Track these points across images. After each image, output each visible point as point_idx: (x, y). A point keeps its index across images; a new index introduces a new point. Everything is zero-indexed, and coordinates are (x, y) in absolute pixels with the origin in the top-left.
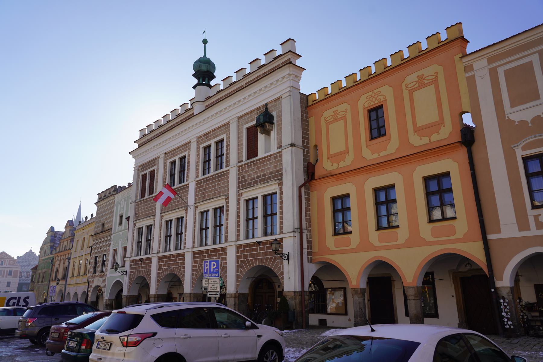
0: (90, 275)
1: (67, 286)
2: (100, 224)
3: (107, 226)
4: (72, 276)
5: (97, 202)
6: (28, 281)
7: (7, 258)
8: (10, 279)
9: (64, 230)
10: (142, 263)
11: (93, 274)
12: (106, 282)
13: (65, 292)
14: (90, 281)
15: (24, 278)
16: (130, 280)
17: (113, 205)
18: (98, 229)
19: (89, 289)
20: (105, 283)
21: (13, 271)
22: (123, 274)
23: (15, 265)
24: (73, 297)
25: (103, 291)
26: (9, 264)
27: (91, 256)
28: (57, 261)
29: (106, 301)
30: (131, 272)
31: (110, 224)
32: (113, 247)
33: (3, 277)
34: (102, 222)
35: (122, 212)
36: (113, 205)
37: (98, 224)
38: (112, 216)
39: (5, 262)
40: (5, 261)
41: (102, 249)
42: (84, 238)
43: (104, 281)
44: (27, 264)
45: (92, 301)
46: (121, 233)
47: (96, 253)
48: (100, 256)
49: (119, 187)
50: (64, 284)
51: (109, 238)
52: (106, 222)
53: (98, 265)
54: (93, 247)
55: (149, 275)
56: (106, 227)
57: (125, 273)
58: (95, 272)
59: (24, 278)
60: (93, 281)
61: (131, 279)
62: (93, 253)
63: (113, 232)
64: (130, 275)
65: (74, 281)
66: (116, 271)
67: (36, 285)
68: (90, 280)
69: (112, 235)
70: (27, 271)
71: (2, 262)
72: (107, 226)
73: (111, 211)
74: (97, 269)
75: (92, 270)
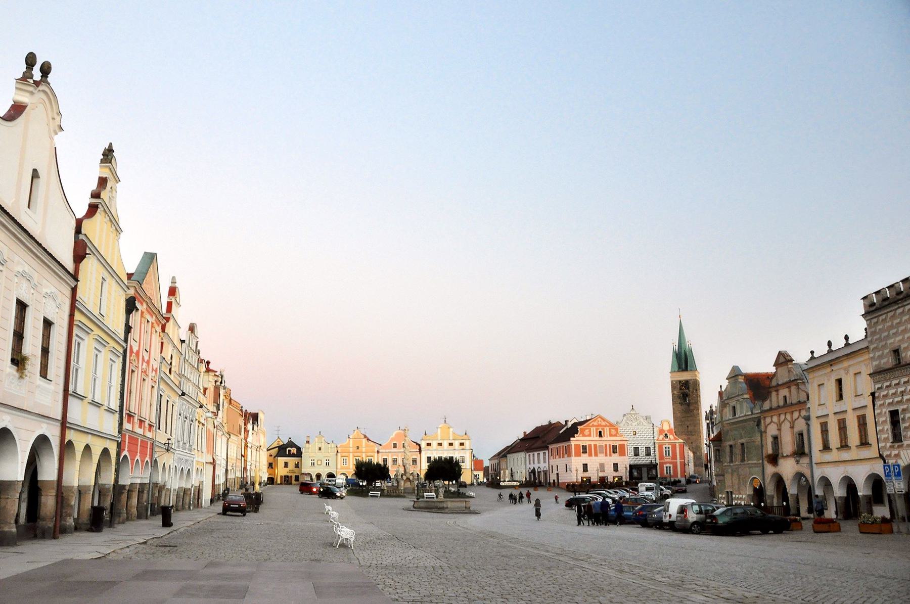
1: (814, 466)
2: (886, 351)
4: (842, 447)
5: (864, 313)
6: (647, 462)
7: (606, 426)
8: (616, 458)
9: (773, 370)
13: (812, 477)
15: (632, 456)
18: (885, 360)
21: (587, 447)
23: (618, 435)
24: (819, 481)
26: (611, 435)
27: (876, 412)
28: (784, 421)
33: (606, 456)
34: (895, 346)
37: (881, 352)
39: (604, 431)
40: (603, 429)
42: (839, 382)
44: (632, 432)
47: (890, 404)
48: (904, 410)
50: (809, 462)
52: (903, 346)
54: (876, 395)
59: (632, 456)
60: (897, 456)
62: (881, 405)
65: (834, 455)
67: (726, 466)
68: (885, 454)
70: (635, 445)
71: (600, 432)
74: (903, 434)
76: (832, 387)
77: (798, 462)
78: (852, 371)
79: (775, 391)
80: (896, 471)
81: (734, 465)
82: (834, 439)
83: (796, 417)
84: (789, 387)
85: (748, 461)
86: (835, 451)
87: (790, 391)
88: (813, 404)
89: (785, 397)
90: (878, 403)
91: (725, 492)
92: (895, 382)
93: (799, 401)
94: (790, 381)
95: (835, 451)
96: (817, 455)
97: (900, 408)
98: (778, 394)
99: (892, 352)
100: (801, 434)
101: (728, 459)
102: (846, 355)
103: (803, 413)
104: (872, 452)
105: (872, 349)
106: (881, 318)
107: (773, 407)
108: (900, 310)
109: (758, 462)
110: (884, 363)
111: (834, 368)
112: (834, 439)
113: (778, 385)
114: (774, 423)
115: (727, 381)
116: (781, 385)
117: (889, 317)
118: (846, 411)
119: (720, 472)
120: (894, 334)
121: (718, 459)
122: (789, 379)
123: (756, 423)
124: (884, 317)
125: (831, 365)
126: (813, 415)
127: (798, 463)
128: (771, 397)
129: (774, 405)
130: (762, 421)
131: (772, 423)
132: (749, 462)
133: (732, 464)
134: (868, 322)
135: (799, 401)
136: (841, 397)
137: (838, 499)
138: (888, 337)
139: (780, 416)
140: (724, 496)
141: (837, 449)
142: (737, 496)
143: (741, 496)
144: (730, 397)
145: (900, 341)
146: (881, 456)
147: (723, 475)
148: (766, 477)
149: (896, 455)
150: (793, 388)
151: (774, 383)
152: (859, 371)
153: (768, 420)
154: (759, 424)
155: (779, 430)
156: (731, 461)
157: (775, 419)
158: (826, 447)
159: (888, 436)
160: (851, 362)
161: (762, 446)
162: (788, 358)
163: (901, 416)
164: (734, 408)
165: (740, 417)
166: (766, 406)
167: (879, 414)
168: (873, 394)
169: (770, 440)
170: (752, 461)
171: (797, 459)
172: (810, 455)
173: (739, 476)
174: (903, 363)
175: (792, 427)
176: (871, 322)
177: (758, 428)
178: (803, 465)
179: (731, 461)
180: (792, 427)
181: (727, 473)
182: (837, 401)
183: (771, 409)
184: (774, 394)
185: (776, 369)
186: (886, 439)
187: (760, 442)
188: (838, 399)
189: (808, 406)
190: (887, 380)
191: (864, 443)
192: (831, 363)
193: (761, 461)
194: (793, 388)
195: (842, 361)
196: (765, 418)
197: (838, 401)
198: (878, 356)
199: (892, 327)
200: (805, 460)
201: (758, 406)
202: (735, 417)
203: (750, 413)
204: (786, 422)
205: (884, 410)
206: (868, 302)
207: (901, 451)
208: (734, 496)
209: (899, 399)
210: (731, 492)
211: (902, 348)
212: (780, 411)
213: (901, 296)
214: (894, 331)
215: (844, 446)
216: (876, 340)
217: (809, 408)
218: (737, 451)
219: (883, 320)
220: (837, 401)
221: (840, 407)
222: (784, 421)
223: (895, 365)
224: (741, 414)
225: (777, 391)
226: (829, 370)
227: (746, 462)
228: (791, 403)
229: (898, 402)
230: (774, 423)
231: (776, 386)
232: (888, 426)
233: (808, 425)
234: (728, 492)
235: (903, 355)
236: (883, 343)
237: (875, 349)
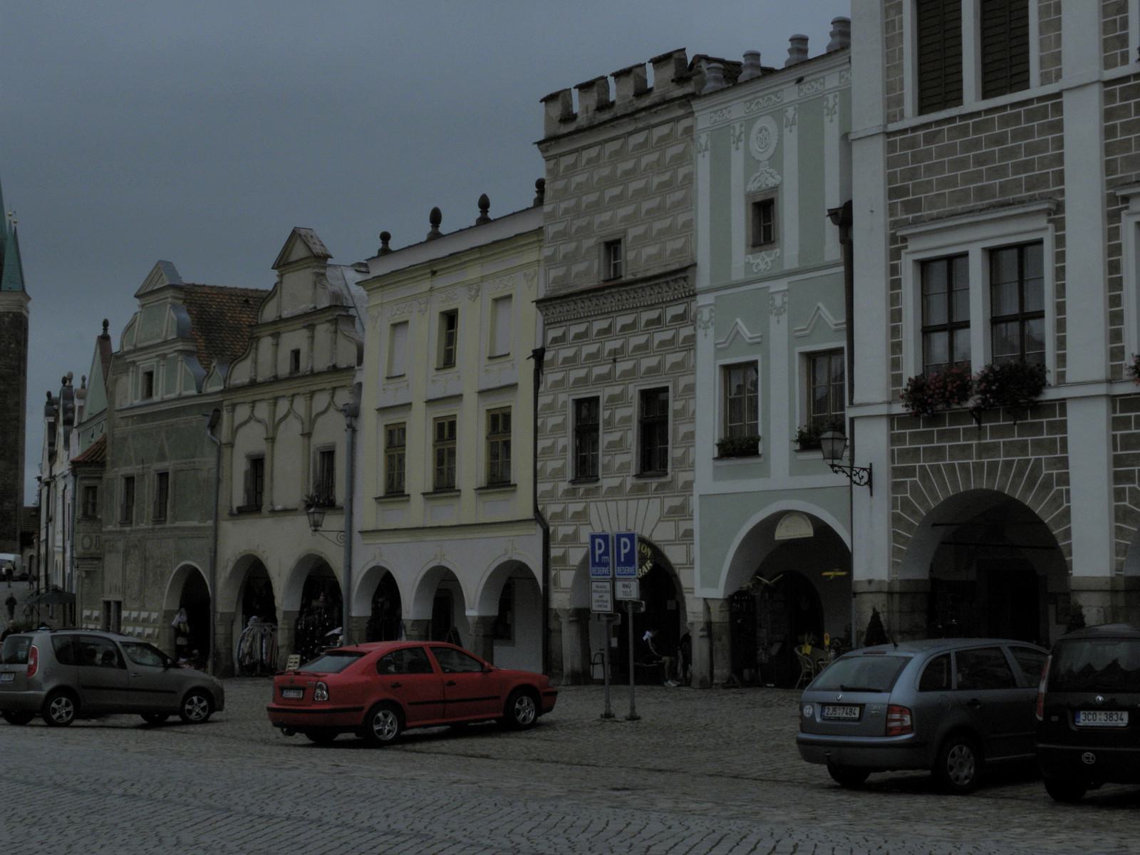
0: (555, 488)
1: (357, 537)
2: (589, 243)
3: (652, 250)
9: (264, 280)
10: (980, 428)
11: (573, 482)
12: (696, 515)
14: (559, 516)
16: (894, 506)
17: (672, 151)
18: (581, 267)
19: (555, 552)
20: (684, 526)
22: (858, 481)
25: (675, 555)
27: (542, 400)
28: (285, 417)
29: (708, 609)
30: (896, 472)
31: (678, 244)
32: (719, 351)
34: (610, 234)
35: (771, 182)
36: (672, 151)
37: (573, 245)
38: (687, 203)
41: (622, 367)
42: (450, 319)
43: (681, 512)
45: (580, 607)
46: (782, 285)
47: (580, 382)
48: (612, 399)
49: (699, 58)
51: (679, 309)
52: (632, 233)
53: (605, 439)
54: (548, 356)
55: (1047, 485)
56: (638, 260)
57: (865, 474)
58: (585, 469)
60: (581, 516)
61: (906, 504)
62: (557, 384)
63: (703, 278)
64: (896, 487)
66: (832, 466)
67: (110, 532)
68: (550, 509)
69: (698, 297)
72: (652, 250)
73: (666, 177)
74: (602, 460)
75: (567, 462)
76: (426, 330)
77: (316, 526)
78: (492, 290)
79: (272, 335)
80: (623, 551)
81: (131, 531)
82: (419, 472)
83: (322, 408)
84: (311, 327)
85: (175, 519)
86: (417, 500)
87: (312, 337)
88: (371, 375)
89: (296, 354)
90: (550, 377)
91: (102, 605)
92: (602, 324)
93: (334, 366)
94: (316, 312)
95: (417, 500)
96: (367, 513)
97: (604, 393)
98: (277, 345)
99: (602, 247)
100: (328, 455)
101: (118, 513)
102: (480, 248)
103: (343, 398)
104: (521, 505)
105: (551, 235)
106: (586, 155)
107: (258, 380)
108: (638, 138)
109: (202, 525)
110: (577, 275)
111: (440, 282)
112: (419, 472)
113: (280, 320)
114: (259, 421)
115: (137, 301)
116: (287, 320)
117: (607, 153)
118: (459, 397)
119: (93, 550)
120: (613, 199)
121: (90, 512)
122: (312, 305)
123: (207, 420)
124: (593, 152)
125: (434, 273)
126: (369, 405)
127: (315, 531)
128: (257, 349)
129: (264, 374)
130: (225, 416)
131: (252, 423)
132: (177, 524)
133: (127, 529)
134: (553, 162)
135: (334, 366)
136: (448, 360)
137: (413, 625)
138: (597, 206)
139: (275, 404)
140: (96, 613)
141: (424, 494)
142: (135, 614)
143: (144, 615)
144: (140, 345)
145: (626, 219)
146: (538, 517)
147: (99, 559)
148: (219, 569)
149: (577, 515)
150: (323, 331)
151: (269, 313)
152: (506, 293)
153: (242, 412)
154: (214, 425)
155: (271, 440)
156: (127, 519)
157: (262, 411)
158: (395, 490)
159: (564, 466)
160: (491, 268)
161: (219, 481)
162: (317, 249)
163: (604, 415)
164: (150, 375)
165: (163, 402)
166: (242, 374)
167: (550, 406)
168: (538, 355)
169: (239, 468)
170: (185, 520)
171: (317, 516)
172: (349, 511)
173: (146, 559)
174: (627, 277)
175: (307, 435)
176: (557, 164)
177: (212, 433)
178: (326, 534)
179: (127, 519)
180: (307, 435)
181: (110, 552)
182: (437, 369)
183: (253, 384)
184: (266, 343)
185: (281, 276)
186: (557, 474)
187: (214, 470)
188: (442, 363)
189: (356, 381)
190: (578, 319)
191: (498, 480)
192: (433, 268)
193: (210, 523)
194: (323, 331)
195: (465, 262)
196: (234, 406)
197: (444, 368)
198: (564, 257)
199: (610, 181)
200: (333, 522)
201: (218, 372)
202: (147, 401)
203: (194, 392)
204: (291, 418)
205: (562, 397)
206: (557, 110)
207: (592, 505)
208: (125, 614)
209: (604, 369)
210: (119, 604)
211: (630, 237)
212: (278, 390)
213: (646, 102)
214: (616, 191)
215: (444, 485)
216: (566, 211)
217: (360, 385)
218: (147, 493)
219: (589, 161)
220: (437, 369)
221: (446, 384)
222: (285, 417)
223: (605, 281)
224: (168, 392)
225: (276, 336)
226: (424, 286)
227: (168, 525)
228: (312, 371)
229: (605, 379)
230: (259, 421)
231: (274, 323)
232: (567, 440)
233: (352, 430)
234: (108, 604)
235: (631, 255)
236: (582, 222)
237: (563, 235)
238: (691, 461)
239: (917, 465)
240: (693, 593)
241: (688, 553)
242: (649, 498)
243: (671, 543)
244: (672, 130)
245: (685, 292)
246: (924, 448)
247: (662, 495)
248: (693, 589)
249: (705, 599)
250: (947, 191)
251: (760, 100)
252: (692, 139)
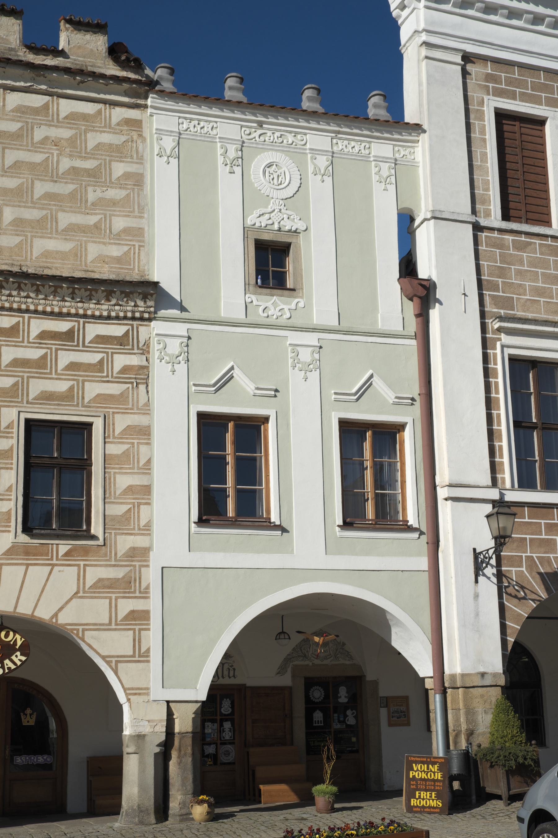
238: (143, 523)
239: (524, 555)
240: (148, 694)
241: (137, 642)
242: (53, 565)
243: (98, 627)
244: (99, 112)
245: (133, 312)
246: (530, 539)
247: (82, 563)
248: (148, 689)
249: (168, 702)
250: (542, 300)
251: (269, 133)
252: (140, 136)
